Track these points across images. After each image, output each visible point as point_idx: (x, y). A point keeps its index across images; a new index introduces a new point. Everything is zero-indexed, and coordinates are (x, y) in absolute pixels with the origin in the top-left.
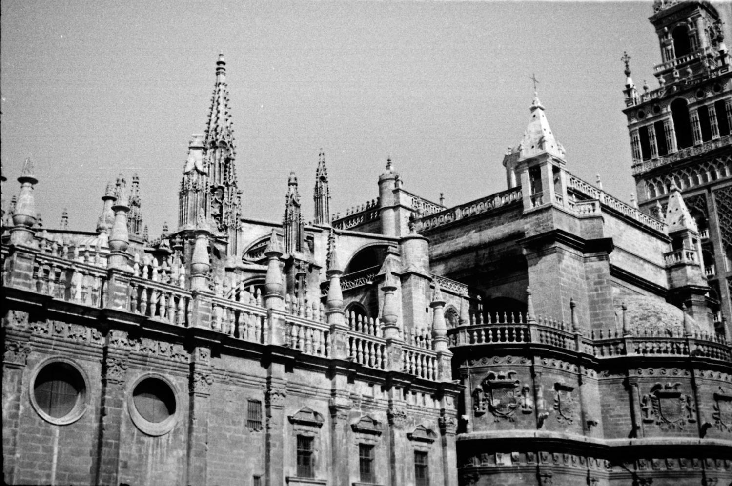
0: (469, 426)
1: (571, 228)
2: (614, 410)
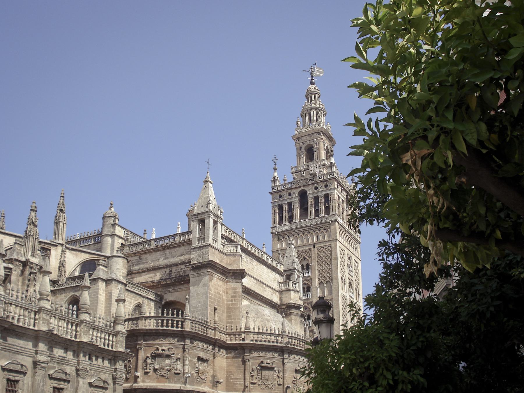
1: (220, 261)
2: (233, 375)
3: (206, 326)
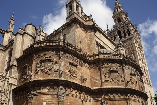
0: (32, 77)
3: (75, 48)
